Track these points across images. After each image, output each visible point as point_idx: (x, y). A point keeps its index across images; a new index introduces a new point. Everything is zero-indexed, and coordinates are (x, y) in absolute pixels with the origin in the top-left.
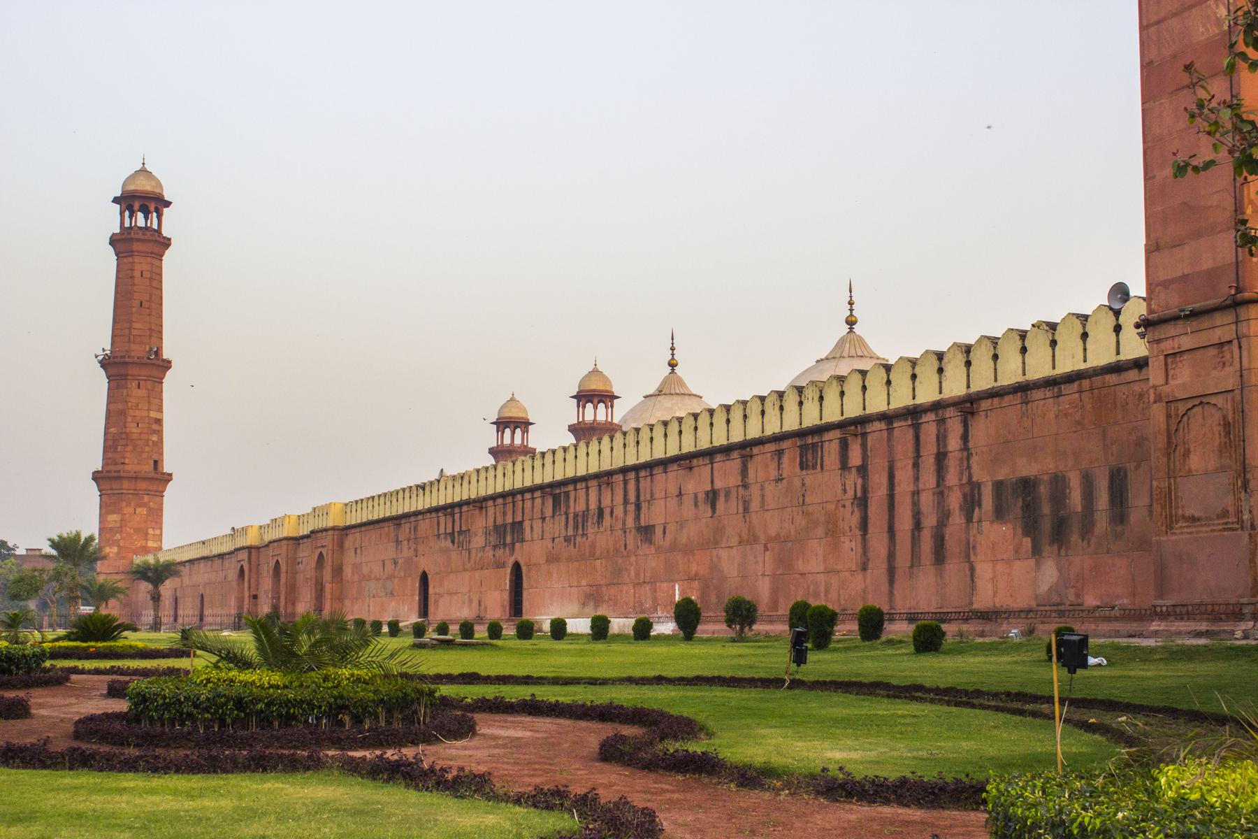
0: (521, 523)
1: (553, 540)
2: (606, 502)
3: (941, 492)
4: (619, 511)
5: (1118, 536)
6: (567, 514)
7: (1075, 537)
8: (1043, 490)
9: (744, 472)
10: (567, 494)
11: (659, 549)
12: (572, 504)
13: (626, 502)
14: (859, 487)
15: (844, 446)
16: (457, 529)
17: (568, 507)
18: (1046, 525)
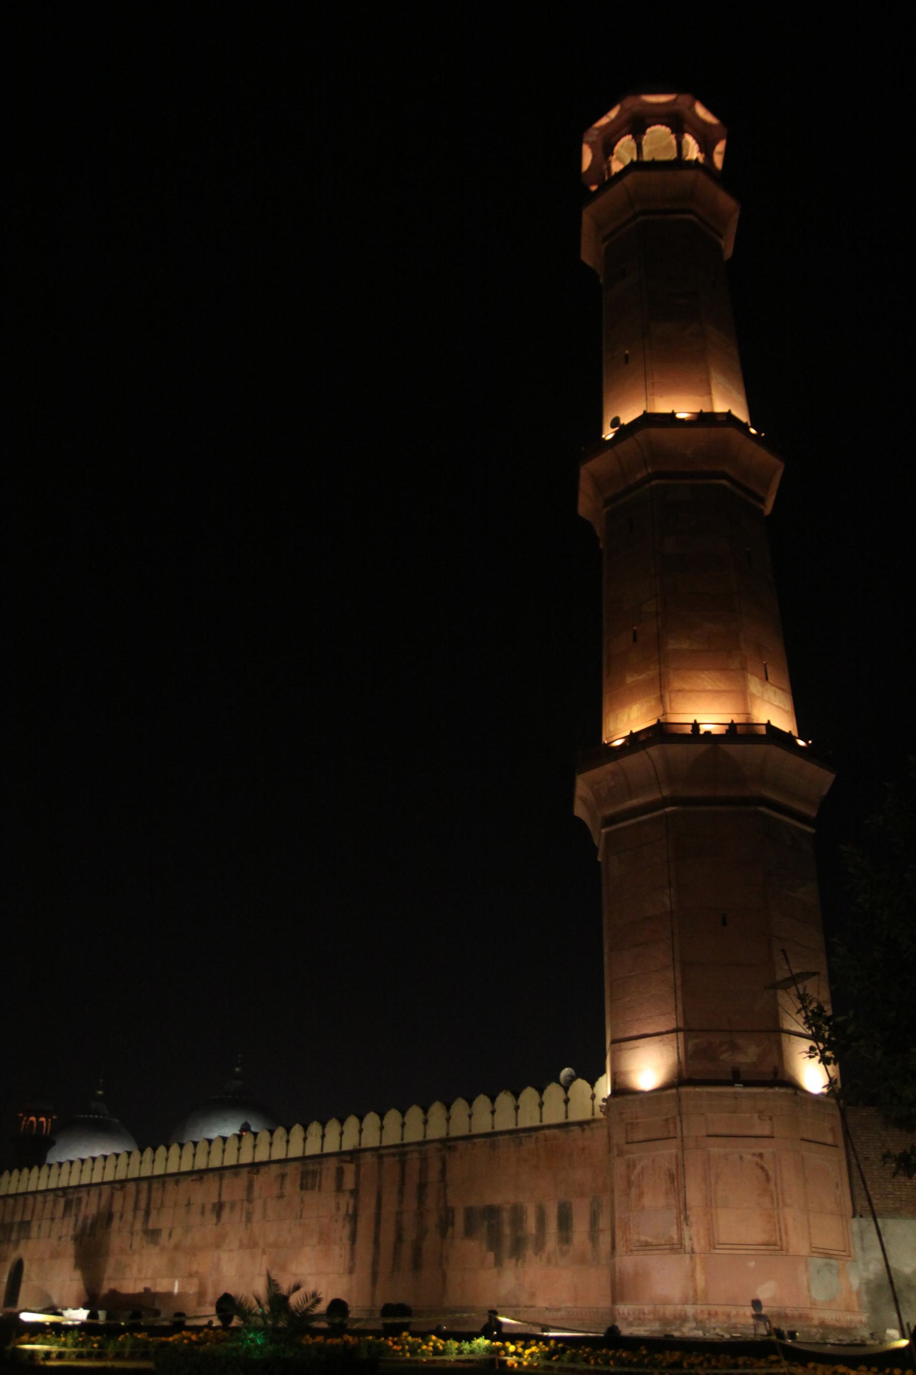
0: (29, 1223)
1: (60, 1238)
3: (421, 1215)
4: (129, 1216)
5: (564, 1254)
6: (77, 1216)
7: (530, 1252)
8: (506, 1216)
9: (250, 1187)
10: (79, 1200)
11: (163, 1249)
12: (83, 1206)
13: (136, 1208)
14: (351, 1206)
15: (340, 1173)
17: (79, 1210)
18: (507, 1243)
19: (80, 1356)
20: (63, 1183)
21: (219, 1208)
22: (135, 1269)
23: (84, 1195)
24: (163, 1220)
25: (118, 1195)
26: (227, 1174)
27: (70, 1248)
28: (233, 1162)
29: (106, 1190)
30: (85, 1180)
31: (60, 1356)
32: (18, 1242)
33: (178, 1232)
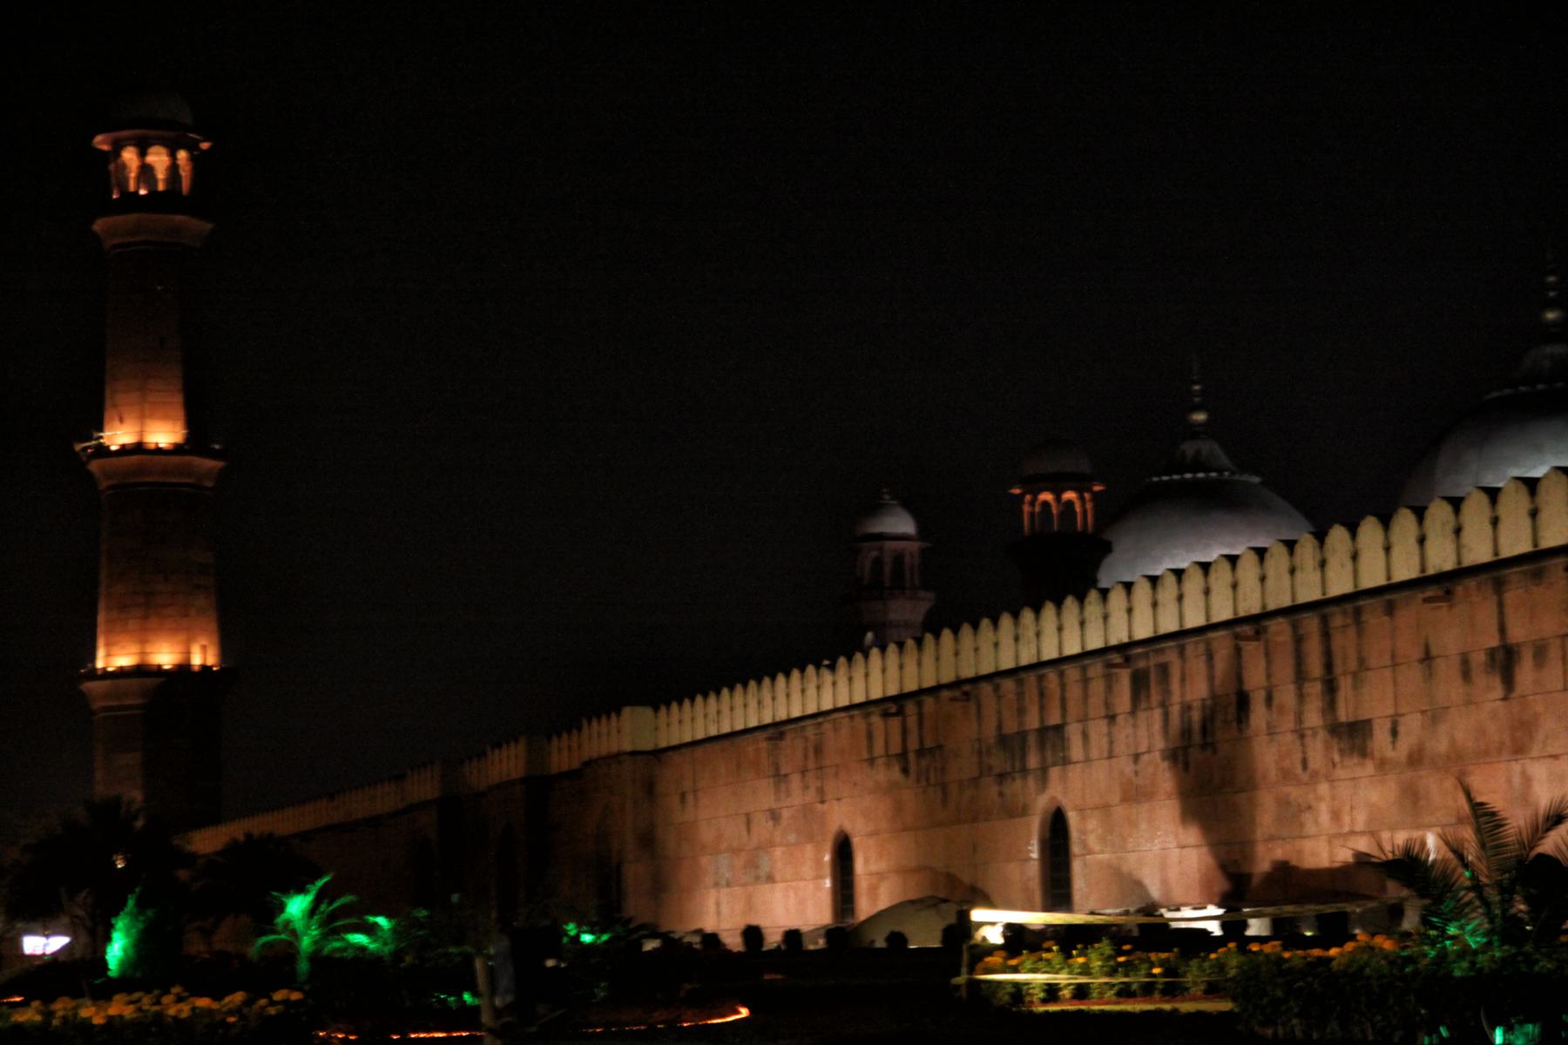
0: (1059, 729)
1: (1136, 757)
2: (1255, 678)
4: (1286, 695)
6: (1164, 705)
10: (1164, 669)
12: (1175, 685)
13: (1300, 676)
16: (913, 744)
17: (1166, 692)
19: (1125, 993)
20: (1119, 635)
21: (1505, 661)
22: (1325, 817)
23: (1171, 657)
24: (1371, 700)
25: (1251, 649)
26: (1512, 573)
27: (1165, 779)
28: (1524, 547)
29: (1222, 643)
30: (1169, 625)
31: (1081, 992)
32: (1044, 771)
33: (1412, 725)
